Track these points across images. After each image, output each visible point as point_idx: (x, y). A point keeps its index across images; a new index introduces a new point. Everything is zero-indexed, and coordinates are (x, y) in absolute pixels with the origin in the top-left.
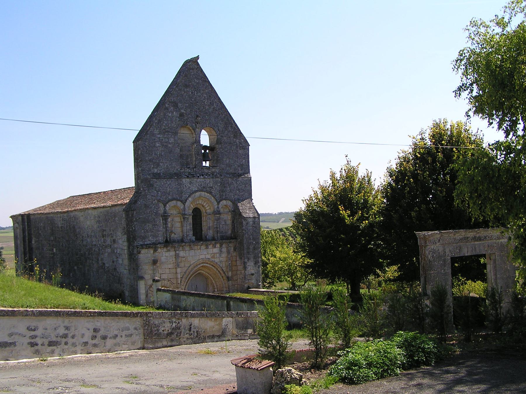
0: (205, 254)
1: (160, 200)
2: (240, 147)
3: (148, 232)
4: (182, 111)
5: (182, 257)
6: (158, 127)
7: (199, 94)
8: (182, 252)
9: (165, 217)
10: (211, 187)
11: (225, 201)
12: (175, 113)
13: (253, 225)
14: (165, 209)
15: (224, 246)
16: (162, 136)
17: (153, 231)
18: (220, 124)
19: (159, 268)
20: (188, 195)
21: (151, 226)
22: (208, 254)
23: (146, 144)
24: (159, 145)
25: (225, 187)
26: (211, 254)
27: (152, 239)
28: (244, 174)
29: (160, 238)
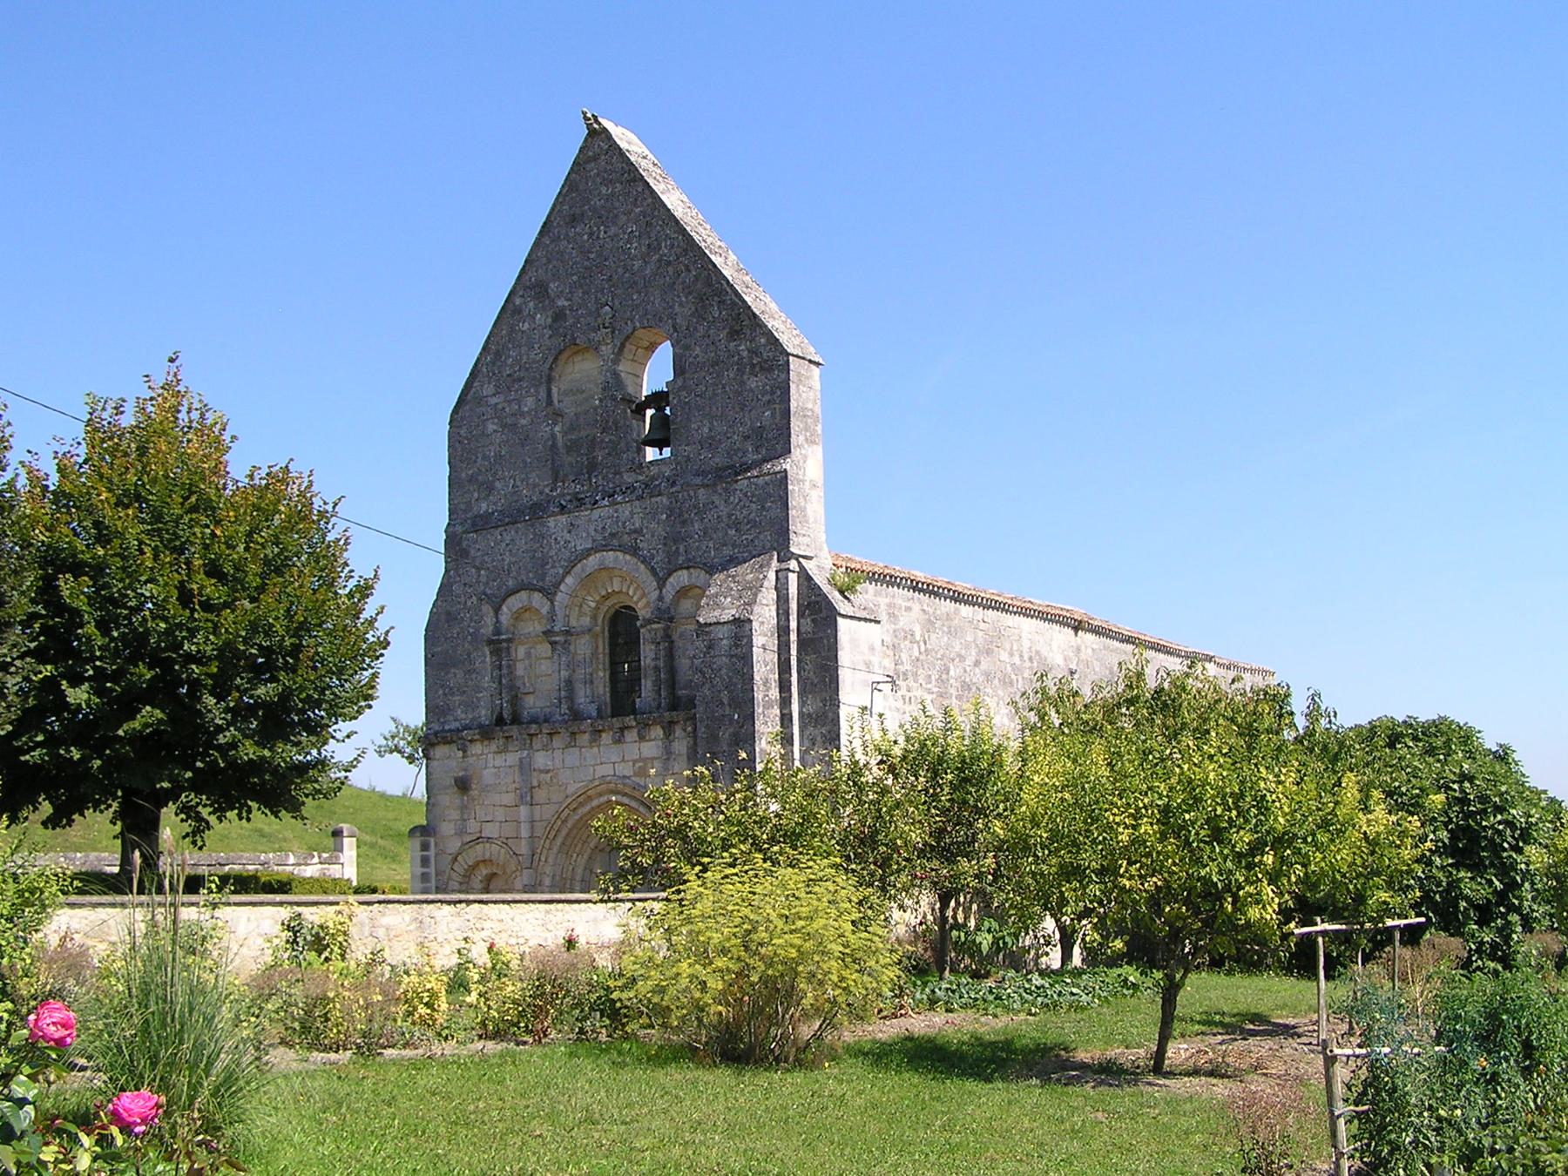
0: (614, 763)
1: (485, 594)
2: (753, 366)
3: (453, 694)
4: (561, 303)
5: (541, 771)
6: (494, 374)
7: (613, 230)
8: (542, 753)
9: (499, 646)
10: (635, 531)
11: (685, 572)
12: (539, 316)
13: (734, 651)
14: (497, 618)
15: (678, 732)
16: (502, 398)
17: (464, 692)
18: (681, 305)
19: (476, 802)
20: (562, 567)
21: (460, 674)
22: (623, 760)
23: (462, 432)
24: (495, 427)
25: (684, 523)
26: (635, 762)
27: (463, 716)
28: (759, 464)
29: (483, 712)
